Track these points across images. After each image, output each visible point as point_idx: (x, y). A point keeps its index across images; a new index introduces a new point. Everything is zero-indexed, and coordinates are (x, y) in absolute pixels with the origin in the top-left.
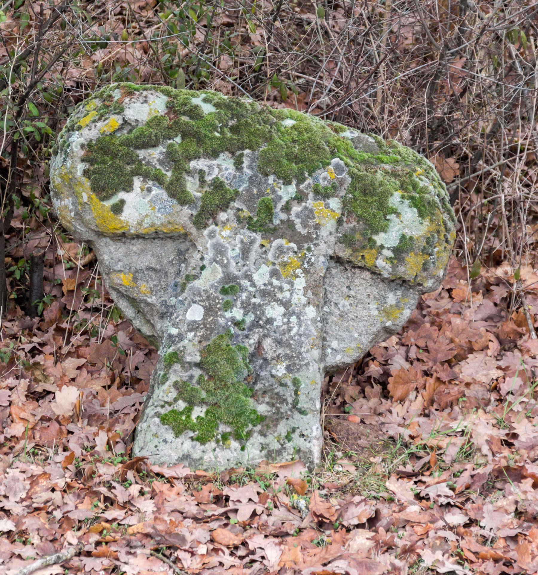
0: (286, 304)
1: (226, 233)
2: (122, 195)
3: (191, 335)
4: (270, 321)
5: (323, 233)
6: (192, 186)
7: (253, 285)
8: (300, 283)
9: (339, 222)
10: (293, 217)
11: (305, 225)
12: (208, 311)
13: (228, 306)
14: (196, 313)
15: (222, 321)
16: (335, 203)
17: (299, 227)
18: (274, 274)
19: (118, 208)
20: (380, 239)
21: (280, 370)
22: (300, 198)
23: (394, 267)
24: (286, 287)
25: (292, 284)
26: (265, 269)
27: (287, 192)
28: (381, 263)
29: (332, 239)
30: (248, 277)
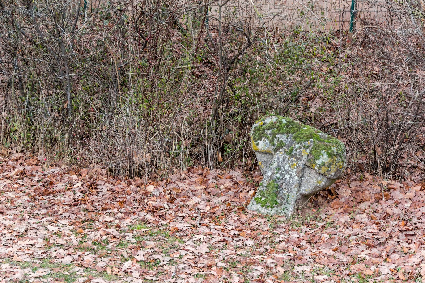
0: (290, 175)
1: (281, 154)
2: (259, 141)
3: (267, 179)
4: (286, 179)
5: (304, 158)
6: (275, 141)
7: (284, 169)
8: (295, 170)
9: (308, 156)
10: (297, 153)
11: (299, 155)
12: (273, 174)
13: (277, 173)
14: (269, 174)
15: (274, 177)
16: (308, 151)
17: (298, 155)
18: (290, 167)
19: (257, 144)
20: (317, 162)
21: (285, 192)
22: (300, 148)
23: (319, 169)
24: (291, 170)
25: (293, 170)
26: (288, 165)
27: (297, 146)
28: (316, 168)
29: (305, 160)
30: (283, 166)
